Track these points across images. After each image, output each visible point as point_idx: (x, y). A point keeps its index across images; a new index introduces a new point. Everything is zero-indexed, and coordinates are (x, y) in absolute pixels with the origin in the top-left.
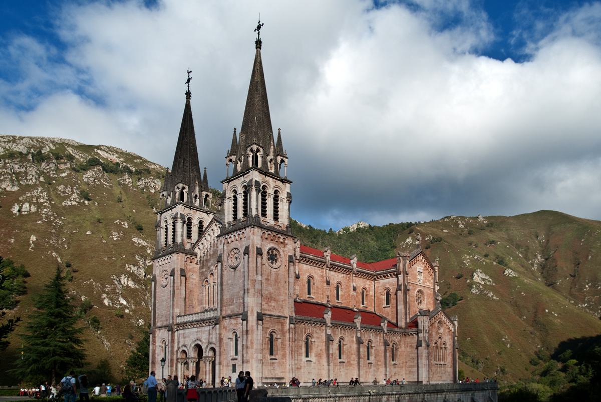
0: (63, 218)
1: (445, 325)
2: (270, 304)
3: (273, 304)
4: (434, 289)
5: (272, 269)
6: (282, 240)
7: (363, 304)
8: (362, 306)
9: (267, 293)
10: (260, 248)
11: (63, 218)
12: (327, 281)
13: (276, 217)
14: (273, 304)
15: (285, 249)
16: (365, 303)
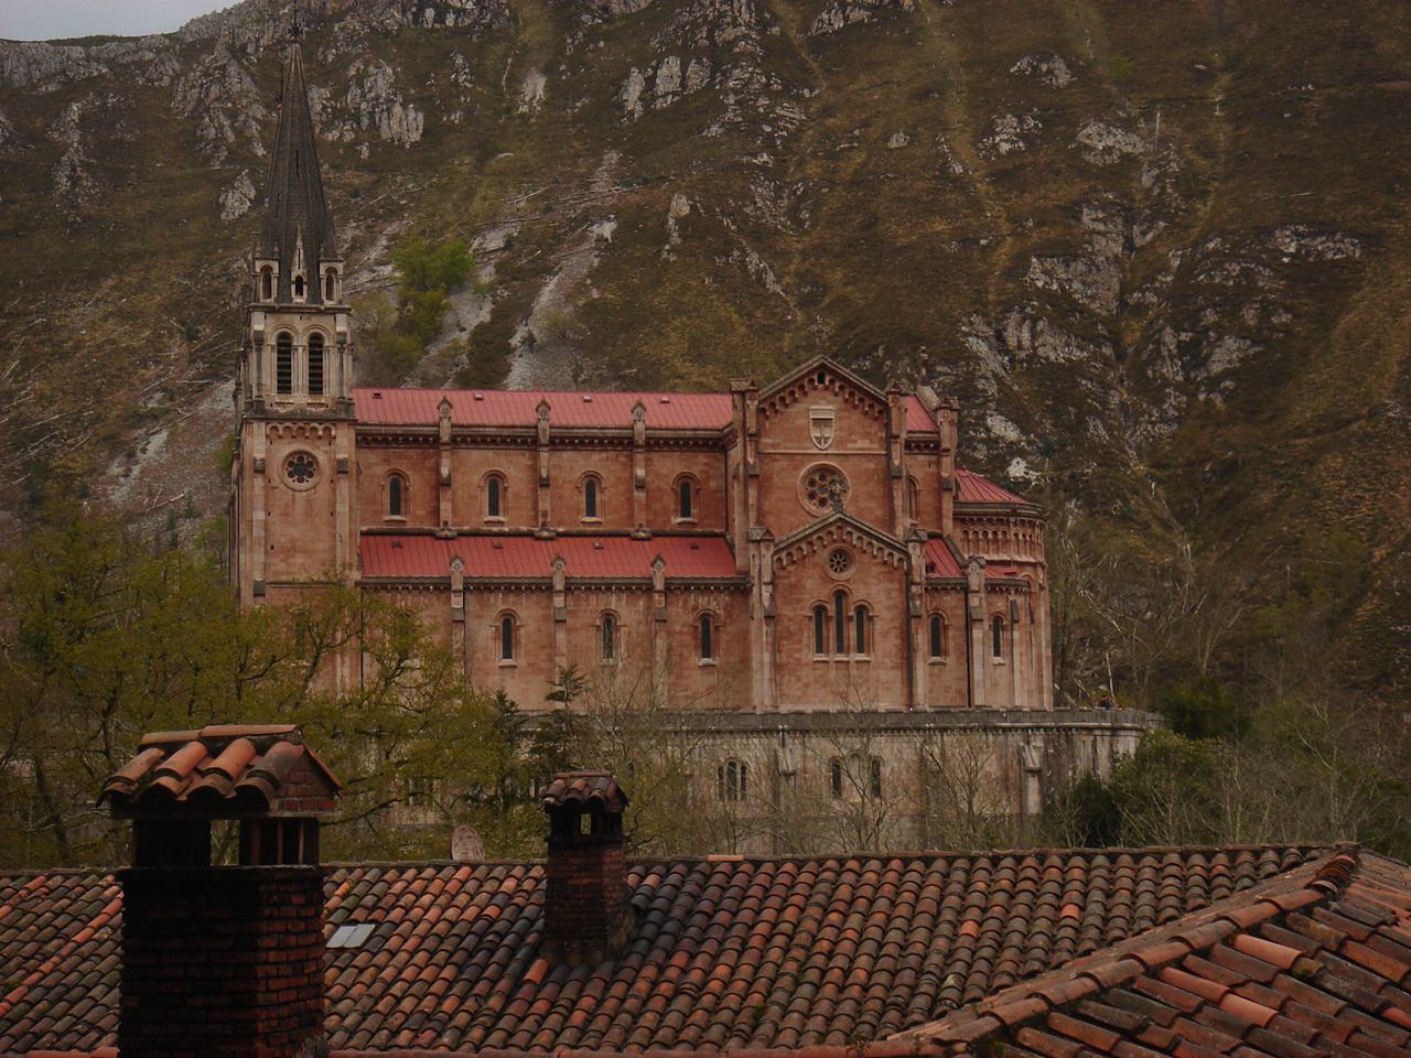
0: (806, 92)
1: (866, 558)
2: (292, 561)
3: (299, 559)
4: (889, 456)
5: (297, 494)
6: (320, 433)
7: (686, 512)
8: (679, 520)
9: (283, 540)
10: (263, 460)
11: (806, 92)
12: (541, 478)
13: (316, 385)
14: (301, 561)
15: (333, 447)
16: (692, 511)
